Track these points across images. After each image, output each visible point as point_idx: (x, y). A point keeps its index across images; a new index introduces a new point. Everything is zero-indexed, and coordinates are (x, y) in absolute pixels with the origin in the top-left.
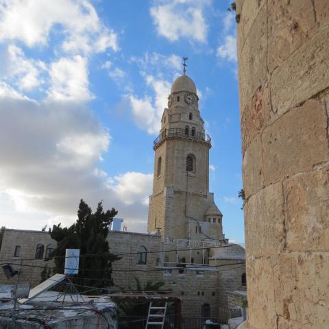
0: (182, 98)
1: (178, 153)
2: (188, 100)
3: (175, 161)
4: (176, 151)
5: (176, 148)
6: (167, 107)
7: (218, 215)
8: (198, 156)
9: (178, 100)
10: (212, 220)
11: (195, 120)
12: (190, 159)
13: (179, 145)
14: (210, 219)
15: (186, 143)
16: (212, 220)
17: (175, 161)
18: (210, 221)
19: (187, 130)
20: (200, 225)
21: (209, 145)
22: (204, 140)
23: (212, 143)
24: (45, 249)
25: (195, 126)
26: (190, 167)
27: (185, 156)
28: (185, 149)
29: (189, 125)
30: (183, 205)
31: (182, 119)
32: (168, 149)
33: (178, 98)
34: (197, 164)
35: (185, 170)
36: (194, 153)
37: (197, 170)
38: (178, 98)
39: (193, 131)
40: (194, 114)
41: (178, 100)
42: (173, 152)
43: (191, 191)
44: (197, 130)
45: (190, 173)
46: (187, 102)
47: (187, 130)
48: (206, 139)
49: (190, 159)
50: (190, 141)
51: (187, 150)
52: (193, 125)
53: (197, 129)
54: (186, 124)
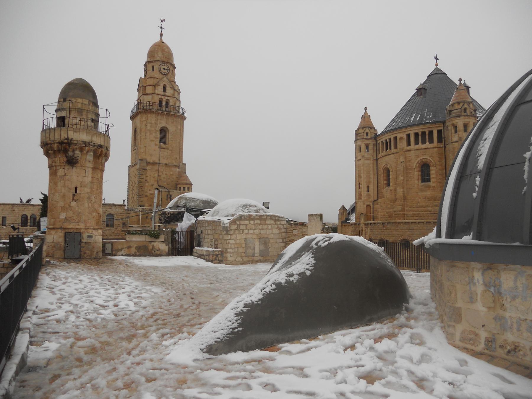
0: (156, 67)
1: (151, 127)
2: (162, 70)
3: (148, 134)
4: (149, 125)
5: (149, 121)
6: (143, 77)
7: (187, 184)
8: (171, 128)
9: (153, 70)
10: (182, 189)
11: (169, 92)
12: (163, 132)
13: (152, 118)
14: (180, 188)
15: (160, 116)
16: (182, 189)
17: (148, 134)
18: (180, 190)
19: (161, 101)
20: (171, 193)
21: (183, 118)
22: (179, 112)
23: (187, 115)
24: (29, 218)
25: (169, 98)
26: (163, 140)
27: (158, 129)
28: (158, 122)
29: (163, 97)
30: (156, 175)
31: (156, 92)
32: (141, 122)
33: (153, 67)
34: (169, 136)
35: (158, 142)
36: (168, 126)
37: (170, 141)
38: (153, 67)
39: (167, 103)
40: (167, 86)
41: (153, 70)
42: (146, 125)
43: (163, 161)
44: (171, 103)
45: (163, 145)
46: (161, 73)
47: (161, 101)
48: (182, 111)
49: (163, 132)
50: (162, 114)
51: (160, 123)
52: (167, 98)
53: (171, 101)
54: (160, 97)
